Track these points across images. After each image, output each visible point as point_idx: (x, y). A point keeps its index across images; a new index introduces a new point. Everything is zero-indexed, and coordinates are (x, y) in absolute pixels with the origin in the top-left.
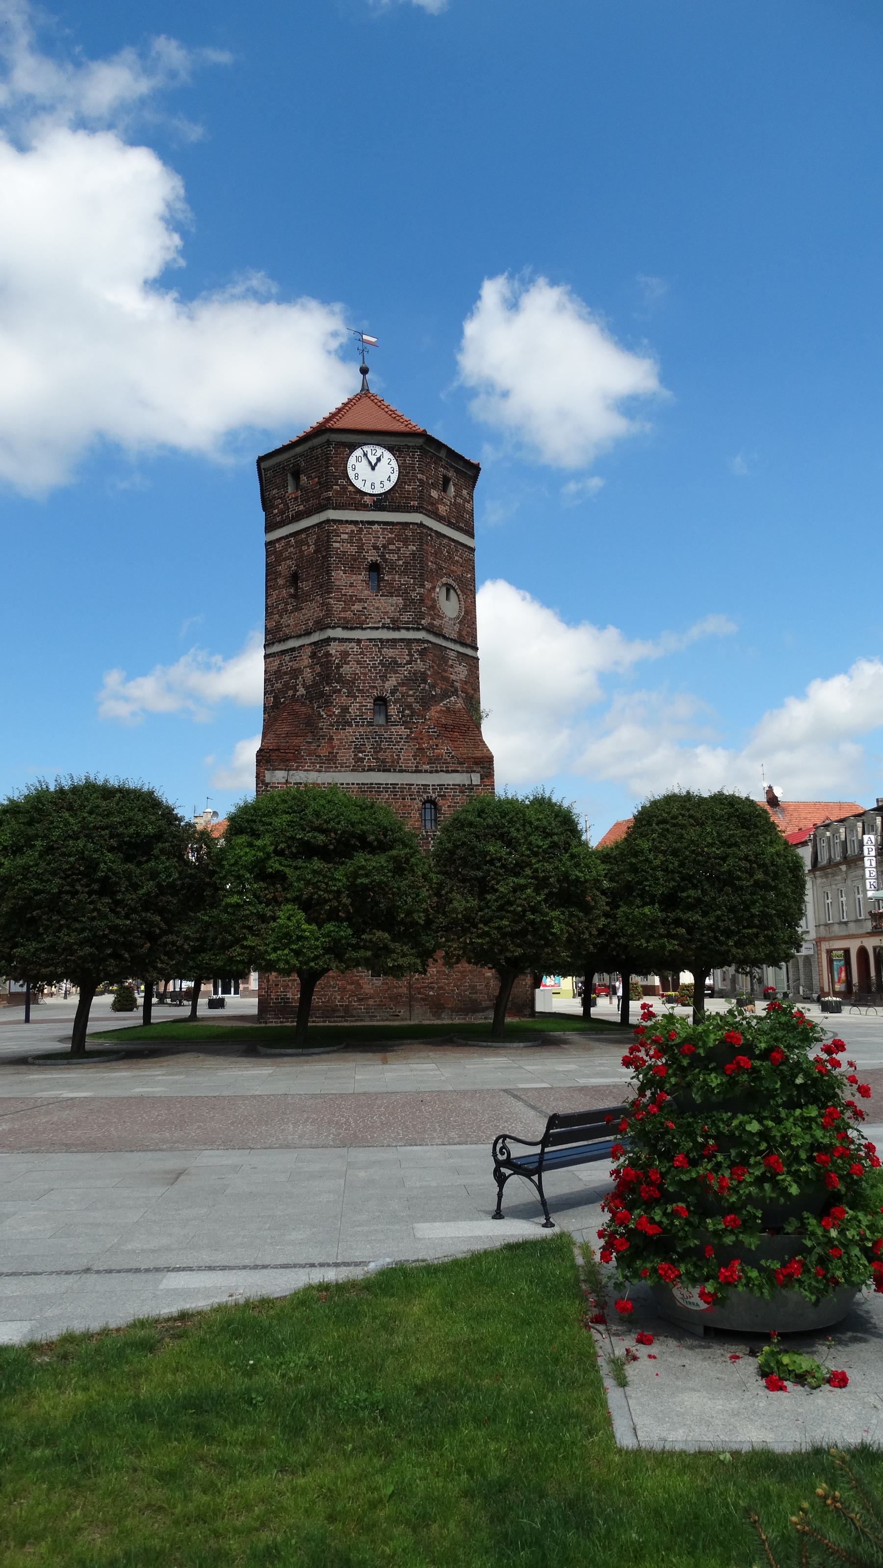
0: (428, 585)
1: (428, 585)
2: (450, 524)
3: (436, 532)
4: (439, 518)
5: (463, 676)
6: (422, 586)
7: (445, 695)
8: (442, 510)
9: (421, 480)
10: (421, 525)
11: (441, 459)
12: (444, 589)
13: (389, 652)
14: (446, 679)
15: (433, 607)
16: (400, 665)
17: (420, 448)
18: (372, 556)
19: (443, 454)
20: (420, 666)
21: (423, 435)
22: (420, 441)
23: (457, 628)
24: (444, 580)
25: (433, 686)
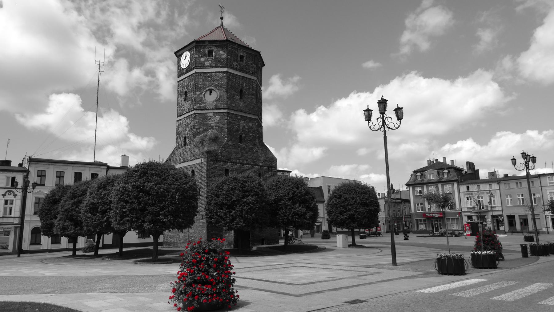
0: (198, 93)
1: (198, 93)
2: (211, 67)
3: (204, 73)
4: (206, 67)
5: (216, 121)
6: (196, 94)
7: (205, 130)
8: (207, 64)
9: (196, 58)
10: (196, 73)
11: (207, 46)
12: (208, 92)
13: (187, 121)
14: (206, 124)
15: (201, 100)
16: (188, 124)
17: (195, 46)
18: (185, 90)
19: (207, 43)
20: (193, 123)
21: (195, 41)
22: (194, 44)
23: (214, 104)
24: (207, 89)
25: (199, 129)
